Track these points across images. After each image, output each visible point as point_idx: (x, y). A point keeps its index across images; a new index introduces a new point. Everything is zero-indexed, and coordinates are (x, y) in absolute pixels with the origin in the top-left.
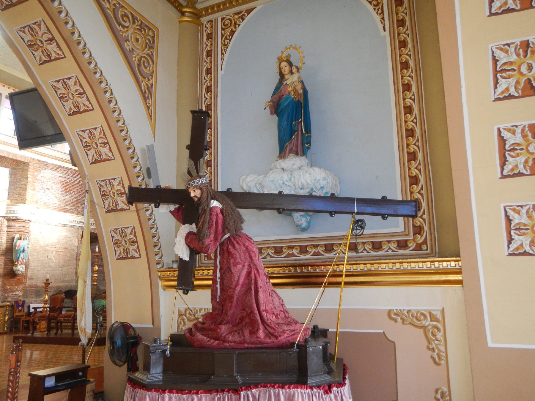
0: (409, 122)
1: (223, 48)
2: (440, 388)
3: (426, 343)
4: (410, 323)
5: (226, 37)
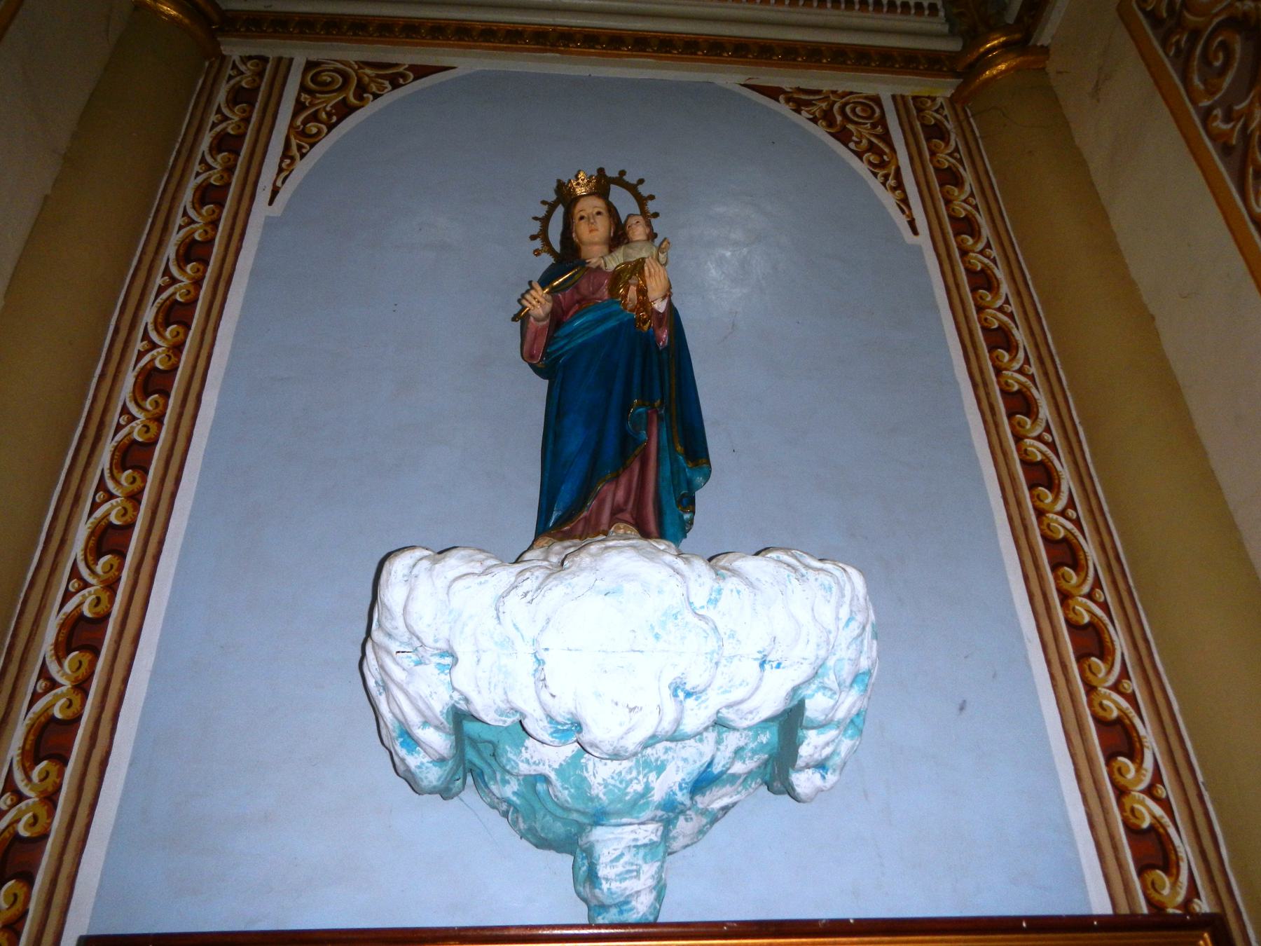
1: (294, 142)
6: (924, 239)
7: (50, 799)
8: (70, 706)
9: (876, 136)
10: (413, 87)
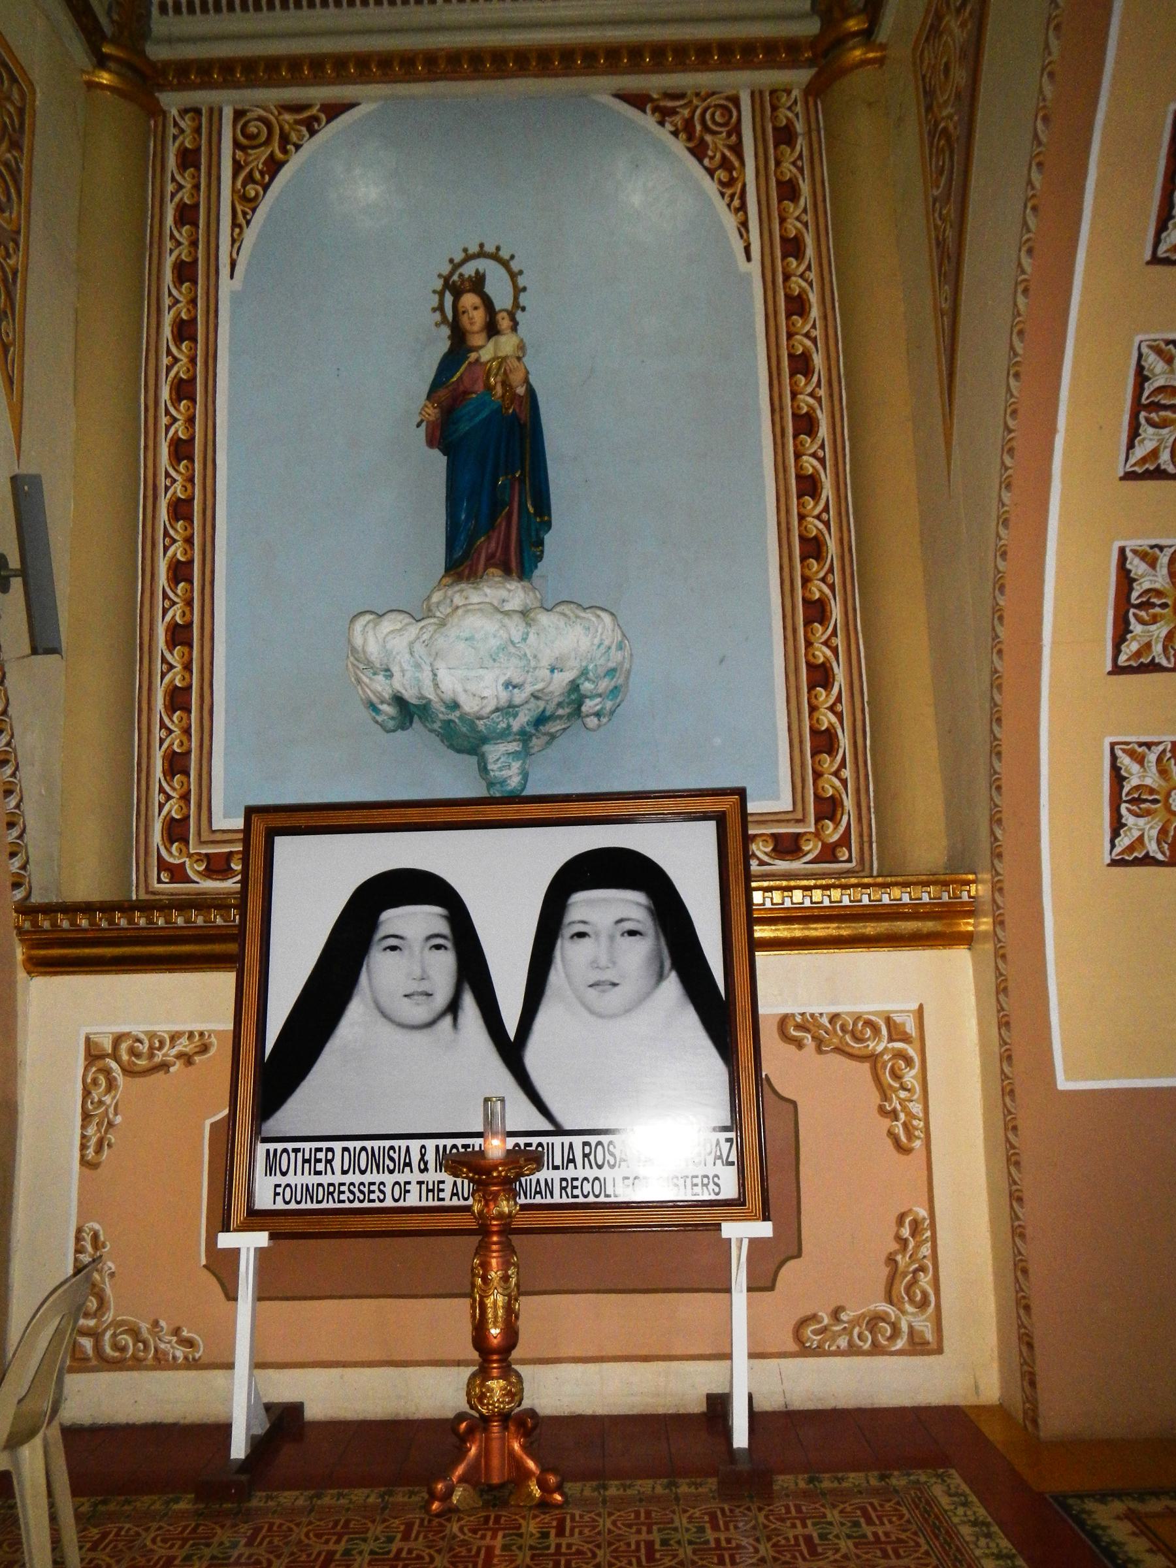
0: (810, 519)
1: (239, 208)
2: (910, 1210)
3: (875, 1098)
4: (838, 1050)
5: (251, 173)
6: (755, 267)
7: (187, 731)
8: (184, 679)
9: (730, 148)
10: (329, 132)
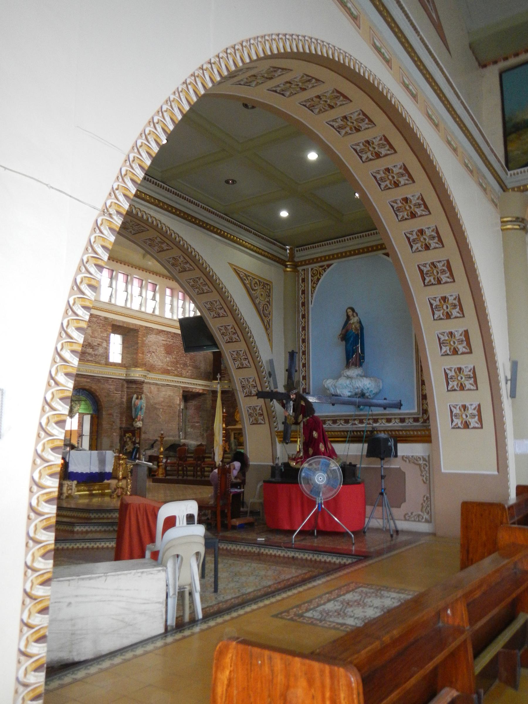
10: (328, 270)
